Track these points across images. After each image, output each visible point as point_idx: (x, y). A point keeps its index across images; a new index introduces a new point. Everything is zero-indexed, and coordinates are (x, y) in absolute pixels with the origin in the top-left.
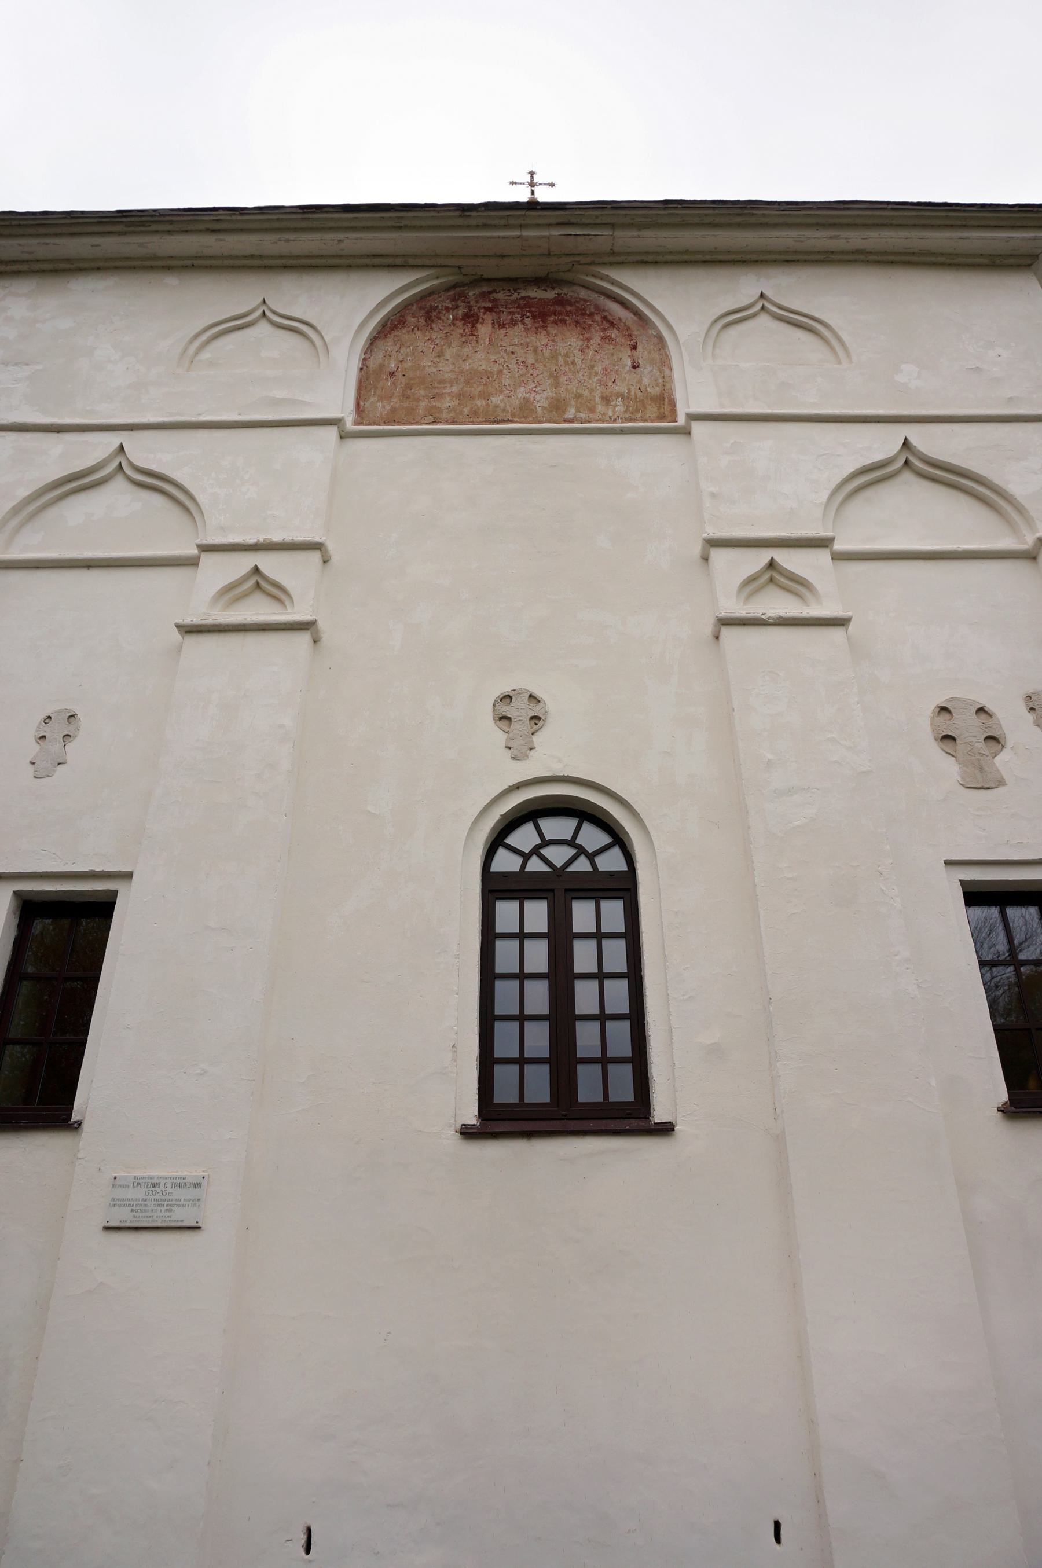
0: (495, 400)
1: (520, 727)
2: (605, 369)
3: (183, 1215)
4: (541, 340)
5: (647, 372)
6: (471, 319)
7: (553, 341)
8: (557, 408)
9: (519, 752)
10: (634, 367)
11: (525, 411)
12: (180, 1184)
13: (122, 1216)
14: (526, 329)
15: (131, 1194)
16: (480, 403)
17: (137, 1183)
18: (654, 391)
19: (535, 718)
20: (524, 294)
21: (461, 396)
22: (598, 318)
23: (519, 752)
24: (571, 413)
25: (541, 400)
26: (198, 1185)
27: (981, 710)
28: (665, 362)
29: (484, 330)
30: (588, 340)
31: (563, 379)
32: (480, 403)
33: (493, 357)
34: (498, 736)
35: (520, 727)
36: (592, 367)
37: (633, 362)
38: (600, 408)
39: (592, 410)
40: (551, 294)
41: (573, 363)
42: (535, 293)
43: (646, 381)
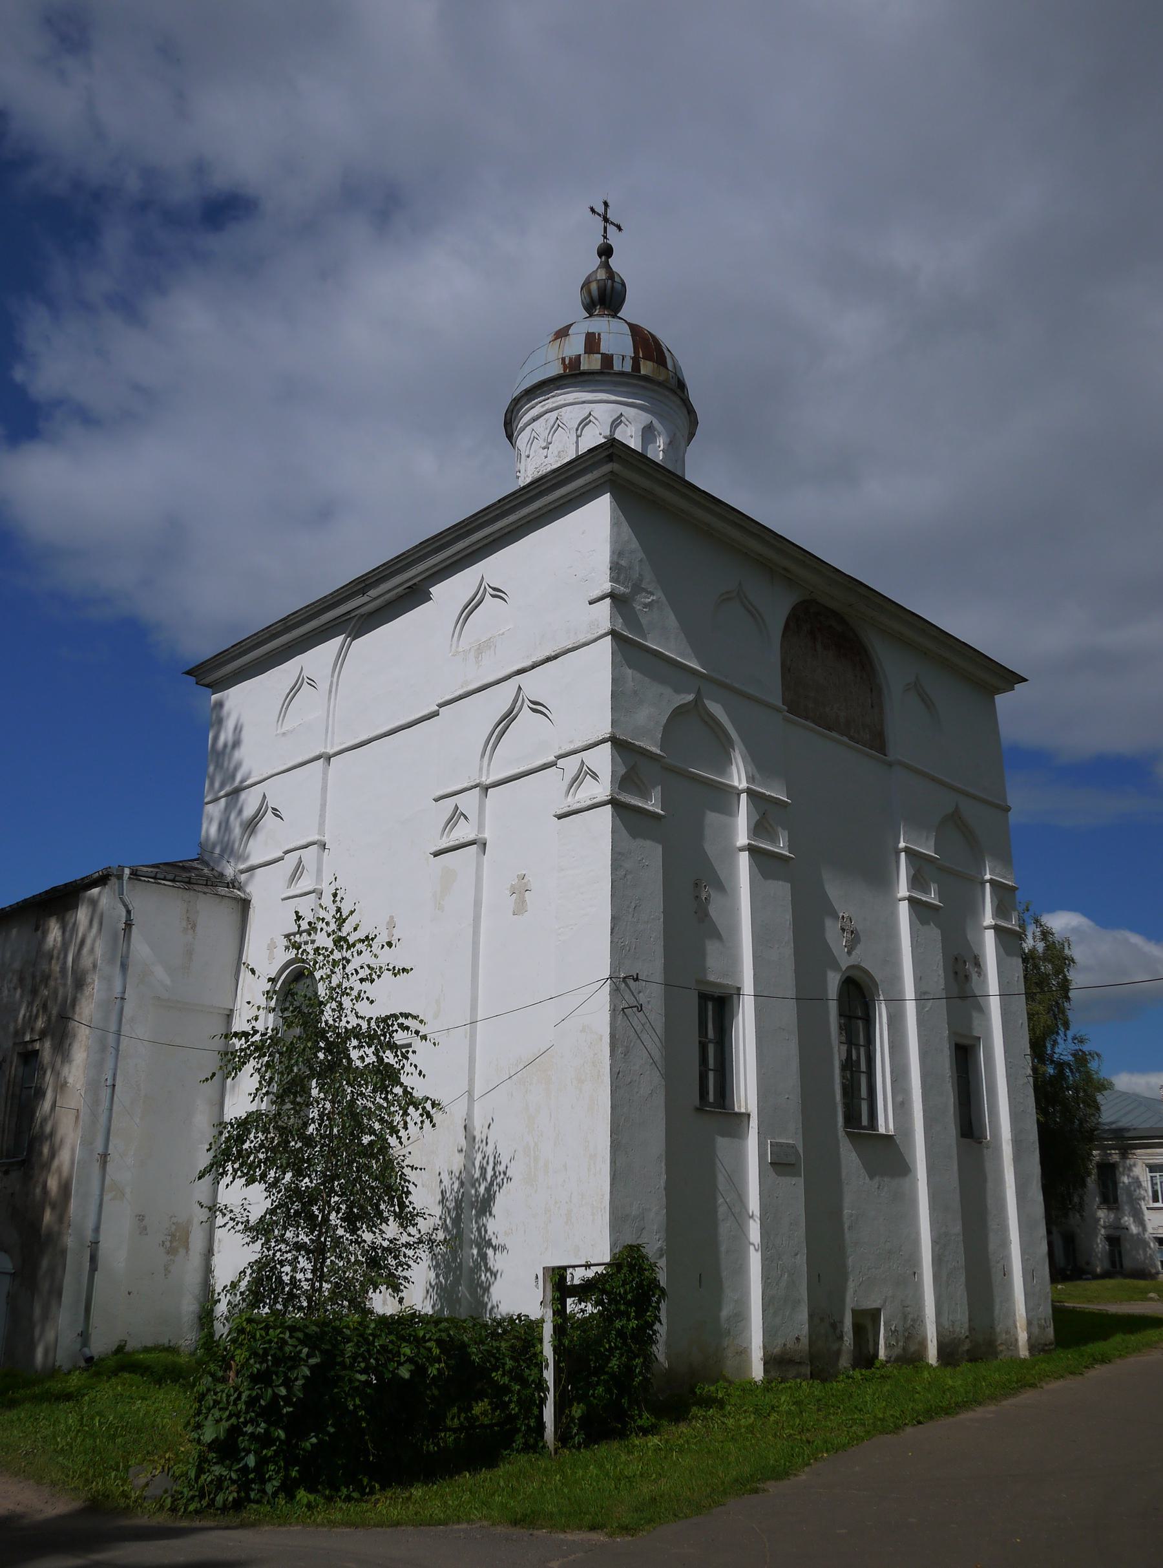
10: (872, 706)
12: (788, 1145)
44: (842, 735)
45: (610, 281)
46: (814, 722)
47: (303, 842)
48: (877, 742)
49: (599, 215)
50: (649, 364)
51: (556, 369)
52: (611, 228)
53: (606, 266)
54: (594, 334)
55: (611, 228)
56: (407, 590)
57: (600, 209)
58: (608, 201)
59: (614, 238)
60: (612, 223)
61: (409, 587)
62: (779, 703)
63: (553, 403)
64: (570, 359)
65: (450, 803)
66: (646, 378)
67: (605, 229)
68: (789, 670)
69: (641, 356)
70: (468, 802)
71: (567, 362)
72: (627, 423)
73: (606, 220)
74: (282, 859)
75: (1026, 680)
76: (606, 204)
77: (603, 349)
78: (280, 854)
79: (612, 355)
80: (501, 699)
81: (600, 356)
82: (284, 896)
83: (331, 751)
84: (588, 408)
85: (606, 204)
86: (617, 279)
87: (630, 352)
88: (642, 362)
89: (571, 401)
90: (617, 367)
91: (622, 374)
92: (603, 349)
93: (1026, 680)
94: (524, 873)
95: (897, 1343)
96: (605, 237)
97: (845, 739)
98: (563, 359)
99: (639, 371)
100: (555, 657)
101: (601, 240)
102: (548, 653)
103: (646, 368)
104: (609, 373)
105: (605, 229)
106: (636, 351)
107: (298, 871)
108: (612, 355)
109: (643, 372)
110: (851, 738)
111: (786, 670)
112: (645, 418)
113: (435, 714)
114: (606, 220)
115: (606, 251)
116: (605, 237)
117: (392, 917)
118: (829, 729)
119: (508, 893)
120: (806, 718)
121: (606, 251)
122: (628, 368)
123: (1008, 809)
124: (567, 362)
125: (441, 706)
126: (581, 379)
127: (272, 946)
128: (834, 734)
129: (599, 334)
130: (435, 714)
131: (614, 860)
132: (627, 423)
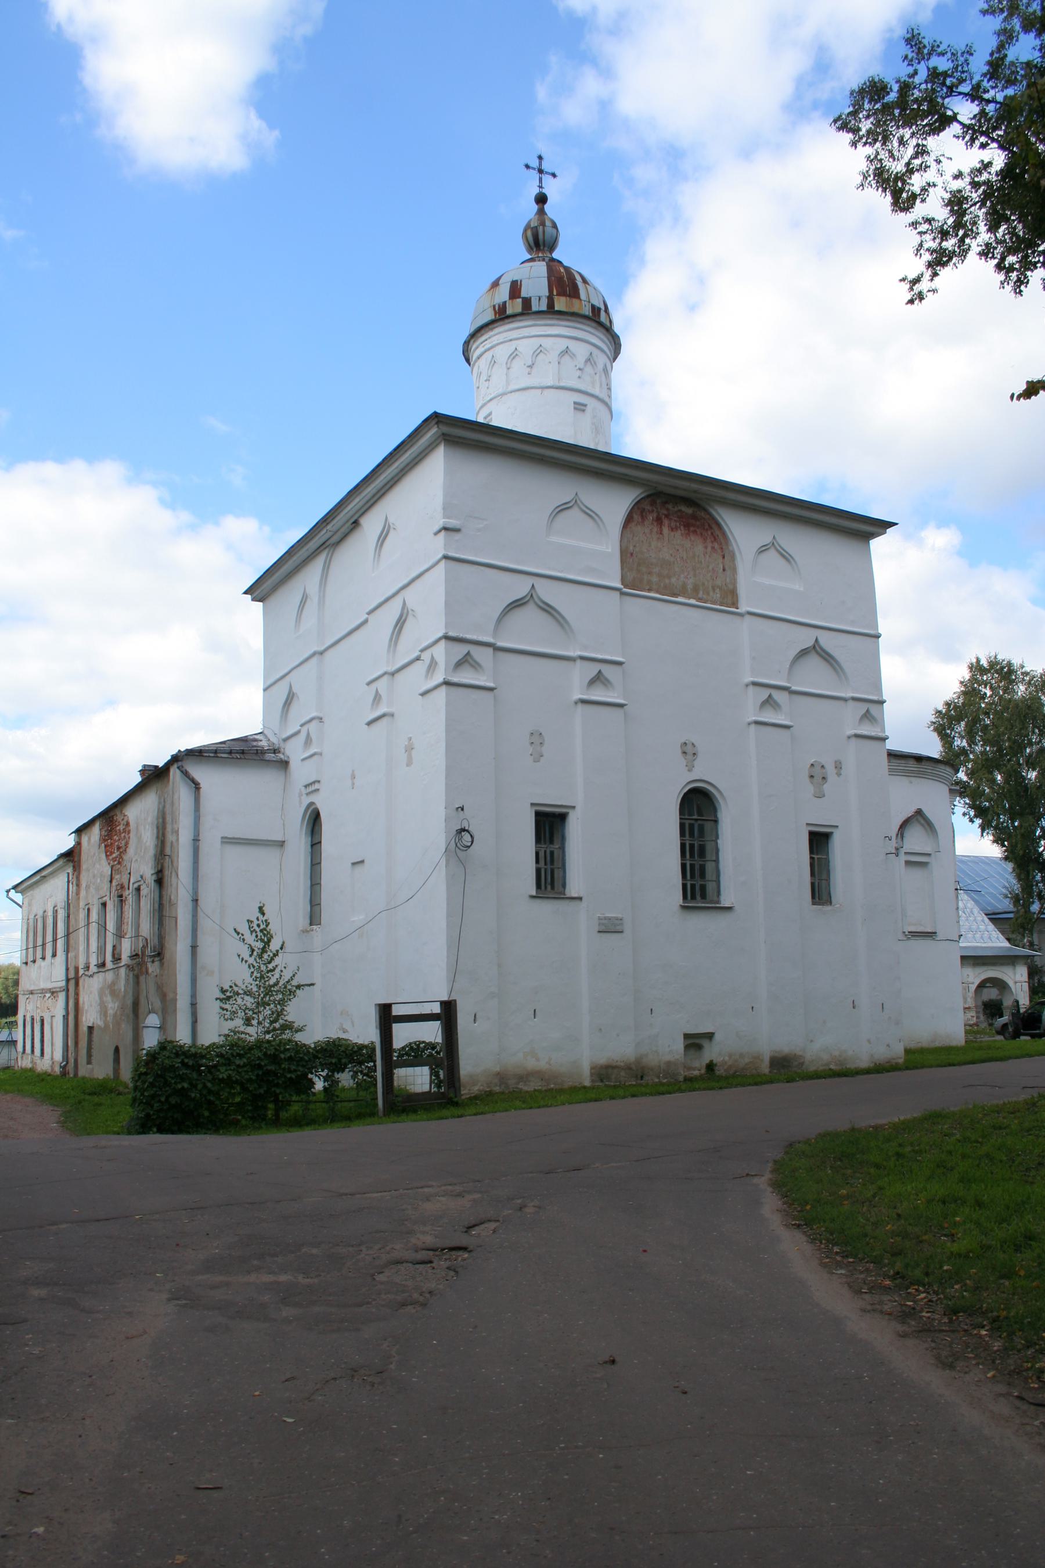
0: (673, 580)
2: (713, 569)
3: (618, 928)
5: (728, 572)
6: (659, 521)
7: (692, 545)
8: (696, 589)
11: (683, 592)
13: (603, 928)
14: (682, 534)
15: (603, 921)
17: (605, 918)
18: (731, 587)
19: (694, 754)
20: (680, 508)
22: (709, 533)
24: (701, 595)
25: (690, 583)
26: (621, 919)
27: (823, 766)
29: (666, 530)
30: (706, 547)
31: (697, 572)
32: (667, 581)
33: (671, 552)
34: (682, 761)
35: (690, 757)
36: (708, 567)
37: (723, 567)
38: (711, 593)
39: (708, 594)
40: (689, 511)
41: (701, 562)
42: (684, 508)
43: (728, 580)
44: (690, 598)
45: (541, 227)
46: (657, 592)
47: (308, 718)
48: (729, 597)
49: (534, 169)
50: (563, 299)
51: (489, 316)
53: (541, 212)
54: (517, 281)
56: (353, 525)
57: (535, 163)
58: (543, 155)
59: (551, 188)
60: (547, 173)
61: (354, 523)
62: (619, 585)
63: (490, 343)
64: (499, 306)
65: (374, 686)
66: (560, 313)
67: (541, 180)
68: (632, 554)
69: (555, 293)
70: (382, 685)
72: (546, 352)
73: (541, 171)
75: (897, 524)
76: (540, 158)
77: (524, 294)
79: (531, 298)
82: (302, 757)
83: (322, 648)
84: (514, 344)
85: (540, 158)
86: (548, 223)
87: (545, 292)
88: (556, 298)
89: (501, 341)
90: (535, 308)
92: (524, 294)
93: (896, 524)
94: (411, 736)
96: (541, 187)
97: (693, 601)
98: (494, 307)
101: (536, 190)
103: (560, 304)
104: (528, 314)
105: (541, 180)
106: (550, 290)
107: (308, 741)
108: (531, 298)
109: (556, 309)
110: (700, 600)
111: (626, 555)
112: (562, 344)
113: (366, 621)
114: (541, 171)
115: (541, 199)
116: (541, 187)
119: (404, 751)
120: (649, 590)
121: (541, 199)
122: (544, 307)
123: (878, 636)
125: (369, 613)
126: (507, 321)
127: (300, 795)
128: (680, 599)
129: (521, 281)
130: (366, 621)
131: (447, 726)
132: (546, 352)
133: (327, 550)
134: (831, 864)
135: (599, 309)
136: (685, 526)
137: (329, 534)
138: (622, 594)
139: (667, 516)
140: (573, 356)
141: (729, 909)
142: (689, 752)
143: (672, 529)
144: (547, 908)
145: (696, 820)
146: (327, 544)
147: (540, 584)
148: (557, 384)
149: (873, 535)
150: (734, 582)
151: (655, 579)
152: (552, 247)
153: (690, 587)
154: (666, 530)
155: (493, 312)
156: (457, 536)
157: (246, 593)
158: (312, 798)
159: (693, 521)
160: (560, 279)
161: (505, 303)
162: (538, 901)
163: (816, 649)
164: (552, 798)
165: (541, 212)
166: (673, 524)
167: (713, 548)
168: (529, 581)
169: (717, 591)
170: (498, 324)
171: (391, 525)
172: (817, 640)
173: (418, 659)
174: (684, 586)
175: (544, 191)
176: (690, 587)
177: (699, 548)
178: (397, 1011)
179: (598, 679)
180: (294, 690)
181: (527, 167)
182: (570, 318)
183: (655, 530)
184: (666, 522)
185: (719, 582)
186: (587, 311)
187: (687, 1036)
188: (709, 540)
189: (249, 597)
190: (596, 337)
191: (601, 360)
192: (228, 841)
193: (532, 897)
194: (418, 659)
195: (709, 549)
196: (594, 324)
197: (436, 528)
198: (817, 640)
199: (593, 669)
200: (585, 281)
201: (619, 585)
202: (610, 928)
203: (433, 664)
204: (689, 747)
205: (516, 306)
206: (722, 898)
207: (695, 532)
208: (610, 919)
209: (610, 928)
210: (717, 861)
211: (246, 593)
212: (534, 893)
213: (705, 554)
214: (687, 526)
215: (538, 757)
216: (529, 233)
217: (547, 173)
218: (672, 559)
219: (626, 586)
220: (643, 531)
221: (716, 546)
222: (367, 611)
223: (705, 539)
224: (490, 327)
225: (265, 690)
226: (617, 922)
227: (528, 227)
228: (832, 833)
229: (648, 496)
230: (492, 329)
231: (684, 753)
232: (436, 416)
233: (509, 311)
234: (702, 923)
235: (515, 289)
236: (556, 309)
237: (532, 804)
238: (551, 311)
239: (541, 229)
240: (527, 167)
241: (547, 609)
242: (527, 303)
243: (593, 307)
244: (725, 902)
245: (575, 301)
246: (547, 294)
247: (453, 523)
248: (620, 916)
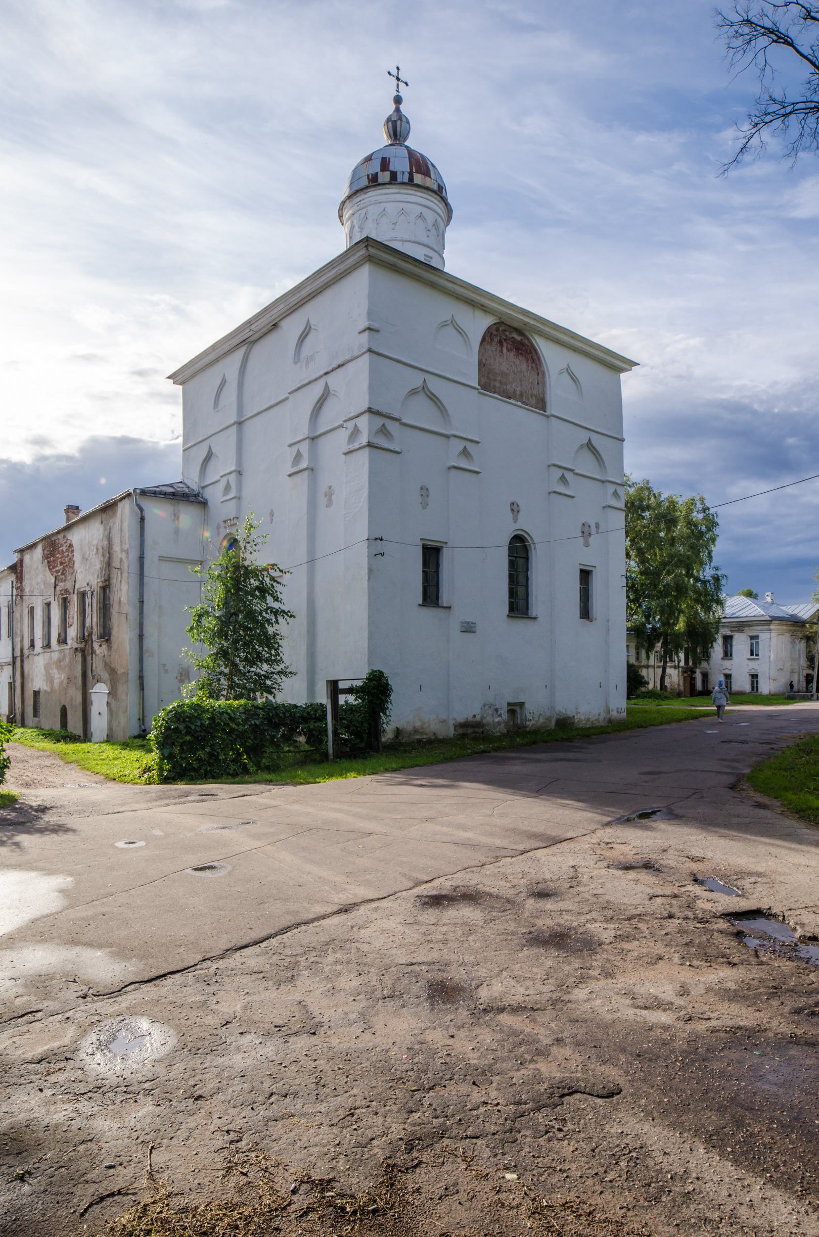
0: (508, 386)
1: (516, 512)
4: (517, 361)
5: (540, 385)
6: (500, 343)
8: (521, 395)
9: (515, 520)
12: (473, 623)
13: (464, 629)
15: (465, 625)
16: (505, 387)
17: (466, 622)
18: (542, 396)
21: (501, 382)
23: (515, 520)
28: (544, 383)
32: (505, 387)
34: (510, 514)
35: (516, 512)
40: (519, 338)
44: (518, 401)
46: (499, 394)
47: (228, 471)
48: (541, 404)
49: (394, 76)
52: (401, 85)
53: (398, 110)
54: (386, 158)
55: (401, 85)
57: (394, 72)
59: (404, 91)
60: (402, 81)
61: (274, 325)
62: (477, 386)
64: (372, 175)
65: (295, 449)
66: (418, 186)
67: (398, 85)
71: (370, 177)
73: (398, 79)
74: (218, 481)
76: (398, 68)
77: (391, 168)
78: (219, 478)
80: (316, 391)
81: (389, 173)
84: (383, 205)
85: (398, 68)
86: (404, 119)
90: (399, 180)
91: (403, 183)
92: (391, 168)
95: (533, 718)
96: (398, 91)
97: (519, 403)
98: (368, 176)
99: (413, 181)
100: (343, 365)
101: (395, 93)
102: (340, 362)
103: (418, 178)
104: (395, 184)
105: (398, 85)
109: (415, 182)
110: (523, 403)
111: (481, 365)
114: (398, 79)
115: (398, 100)
116: (398, 91)
117: (272, 510)
118: (509, 398)
120: (495, 392)
121: (398, 100)
122: (406, 180)
123: (623, 440)
124: (370, 177)
126: (378, 188)
128: (512, 401)
133: (246, 346)
134: (590, 592)
135: (442, 188)
136: (516, 349)
137: (252, 333)
138: (479, 393)
139: (505, 340)
140: (424, 220)
141: (535, 618)
142: (515, 508)
143: (508, 350)
144: (429, 613)
145: (516, 557)
146: (247, 341)
147: (429, 378)
148: (414, 239)
149: (622, 370)
150: (544, 393)
151: (498, 385)
152: (405, 139)
153: (518, 393)
154: (505, 350)
155: (367, 180)
156: (377, 336)
157: (168, 378)
158: (234, 531)
159: (521, 347)
160: (417, 161)
161: (377, 174)
162: (424, 608)
163: (590, 446)
164: (435, 535)
165: (398, 110)
166: (509, 346)
167: (532, 367)
168: (423, 376)
169: (534, 398)
170: (372, 189)
171: (312, 327)
172: (590, 440)
173: (341, 426)
174: (515, 392)
175: (400, 94)
176: (518, 393)
177: (524, 366)
178: (342, 685)
179: (465, 453)
180: (214, 450)
181: (389, 73)
182: (424, 191)
183: (498, 349)
184: (505, 344)
185: (535, 392)
186: (435, 187)
187: (509, 704)
188: (530, 361)
189: (171, 381)
190: (439, 207)
191: (441, 224)
192: (162, 559)
193: (420, 605)
194: (341, 426)
195: (530, 367)
196: (439, 198)
197: (362, 327)
198: (590, 440)
199: (461, 445)
200: (433, 166)
201: (477, 386)
202: (468, 628)
203: (356, 432)
204: (515, 505)
205: (385, 177)
206: (530, 612)
207: (522, 354)
208: (468, 623)
209: (468, 628)
210: (527, 586)
211: (168, 378)
212: (421, 603)
213: (527, 370)
214: (517, 349)
215: (425, 505)
216: (390, 124)
217: (402, 81)
218: (508, 372)
219: (482, 389)
220: (493, 348)
221: (534, 366)
222: (290, 391)
223: (527, 360)
224: (365, 191)
225: (184, 451)
226: (472, 625)
227: (389, 120)
228: (592, 571)
229: (495, 324)
230: (366, 193)
231: (512, 510)
232: (367, 240)
233: (380, 180)
234: (521, 626)
235: (385, 164)
236: (415, 182)
237: (421, 539)
238: (411, 182)
239: (398, 123)
240: (389, 73)
241: (433, 398)
242: (394, 176)
243: (438, 184)
244: (534, 615)
245: (427, 178)
246: (409, 171)
247: (375, 325)
248: (474, 622)
